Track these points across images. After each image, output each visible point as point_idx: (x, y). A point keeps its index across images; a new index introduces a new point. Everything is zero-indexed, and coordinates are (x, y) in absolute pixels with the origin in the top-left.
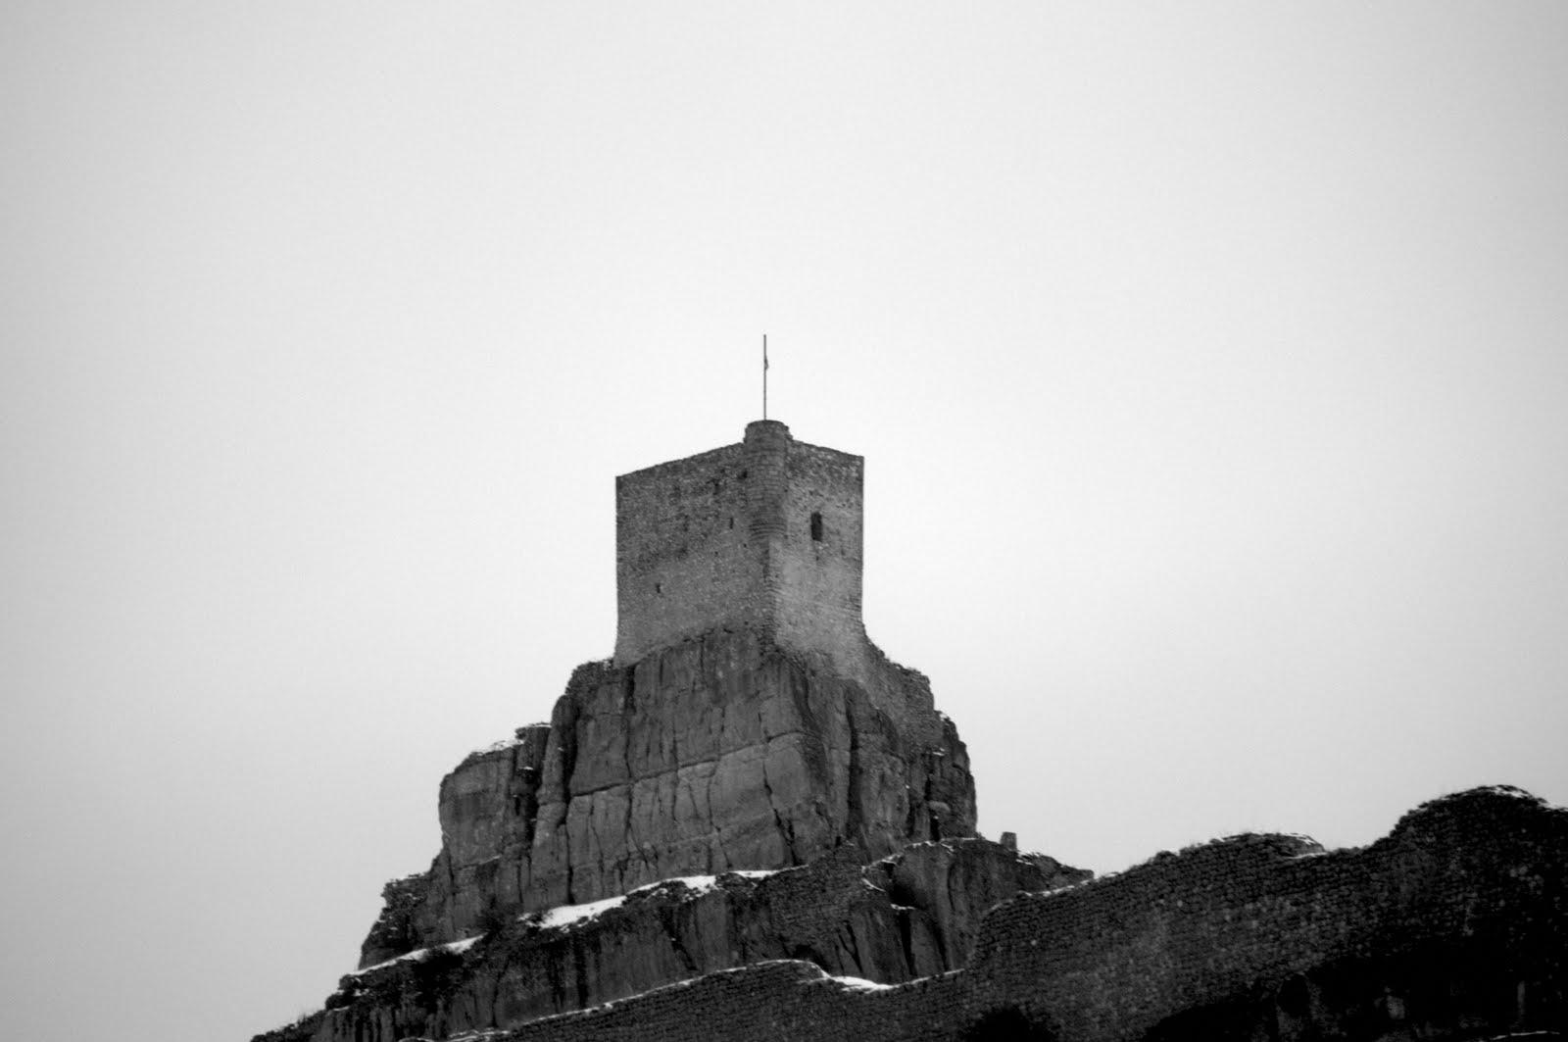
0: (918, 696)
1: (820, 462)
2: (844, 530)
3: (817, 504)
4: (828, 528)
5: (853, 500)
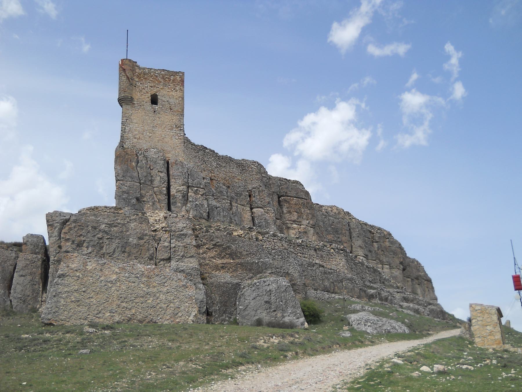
2: (171, 101)
4: (162, 100)
5: (177, 88)
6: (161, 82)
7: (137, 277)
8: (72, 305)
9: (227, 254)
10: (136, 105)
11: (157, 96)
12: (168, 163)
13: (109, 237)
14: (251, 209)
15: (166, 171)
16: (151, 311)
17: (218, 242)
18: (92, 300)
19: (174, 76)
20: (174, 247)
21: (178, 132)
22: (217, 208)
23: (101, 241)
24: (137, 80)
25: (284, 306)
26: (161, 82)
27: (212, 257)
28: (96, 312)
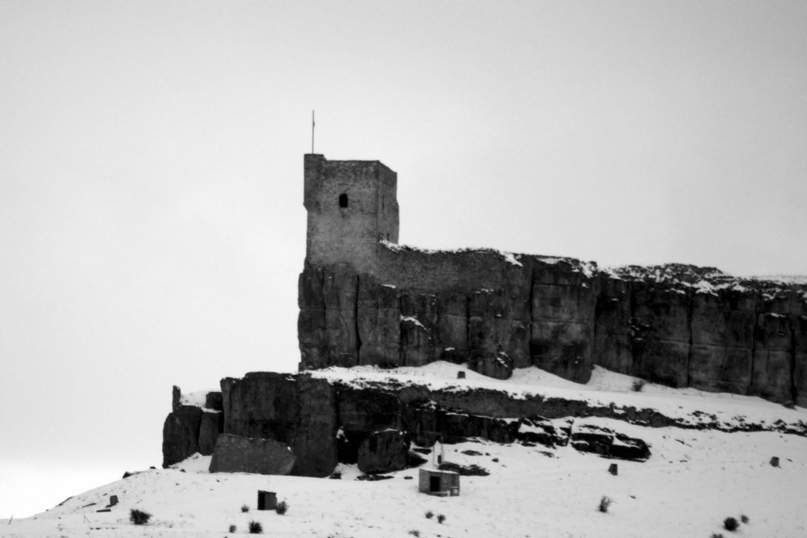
0: (472, 264)
1: (346, 168)
3: (344, 189)
4: (352, 200)
6: (350, 177)
19: (366, 166)
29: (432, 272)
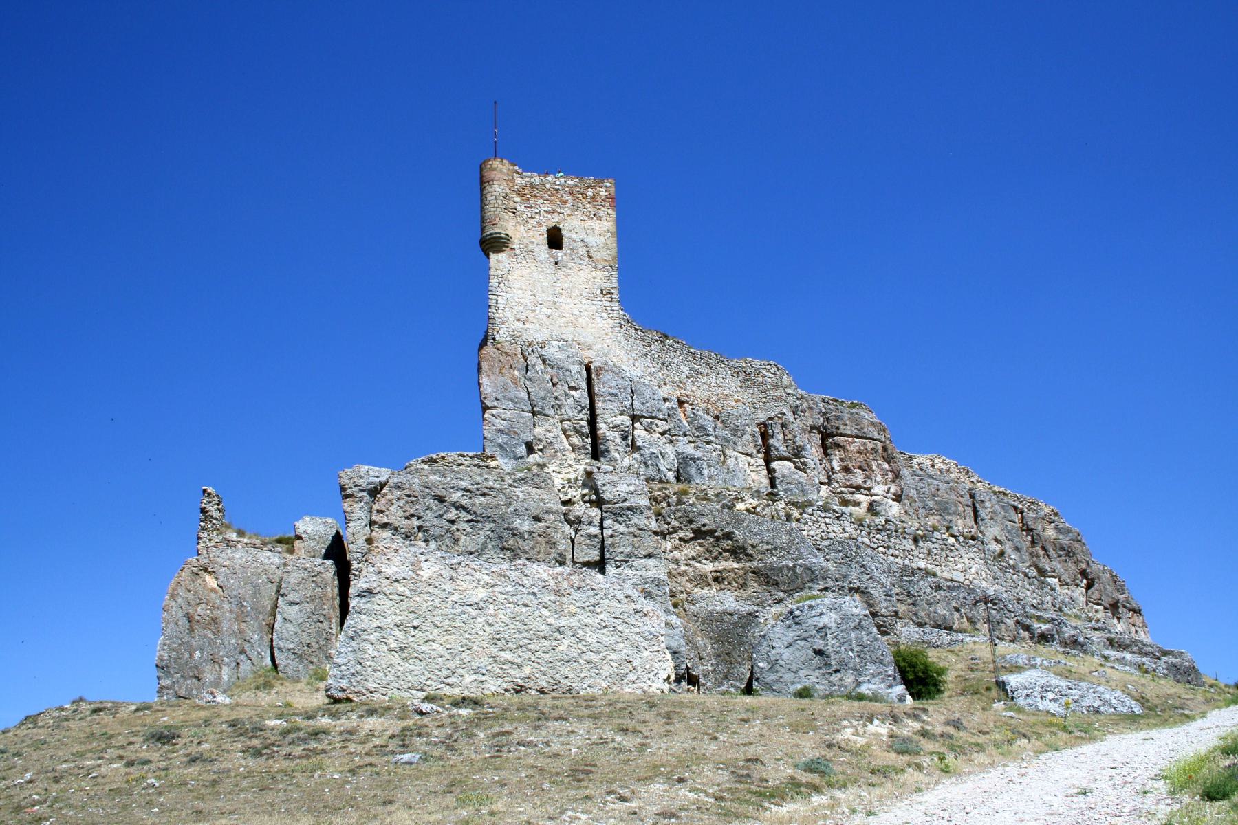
2: (590, 239)
3: (556, 220)
5: (601, 214)
6: (566, 202)
7: (534, 594)
8: (395, 658)
9: (726, 551)
10: (517, 252)
11: (559, 230)
12: (588, 369)
13: (470, 517)
14: (768, 461)
15: (584, 386)
16: (567, 670)
17: (704, 525)
18: (434, 646)
20: (612, 536)
21: (608, 304)
22: (694, 460)
23: (454, 528)
24: (517, 199)
25: (858, 660)
26: (566, 202)
27: (693, 558)
28: (445, 673)
29: (706, 379)
